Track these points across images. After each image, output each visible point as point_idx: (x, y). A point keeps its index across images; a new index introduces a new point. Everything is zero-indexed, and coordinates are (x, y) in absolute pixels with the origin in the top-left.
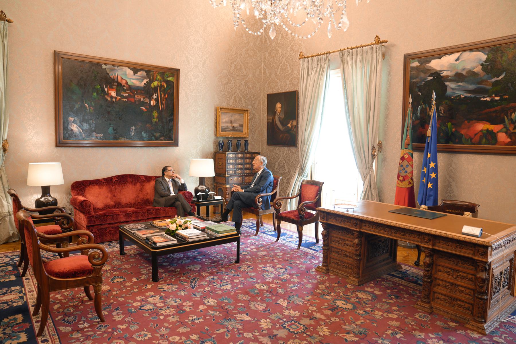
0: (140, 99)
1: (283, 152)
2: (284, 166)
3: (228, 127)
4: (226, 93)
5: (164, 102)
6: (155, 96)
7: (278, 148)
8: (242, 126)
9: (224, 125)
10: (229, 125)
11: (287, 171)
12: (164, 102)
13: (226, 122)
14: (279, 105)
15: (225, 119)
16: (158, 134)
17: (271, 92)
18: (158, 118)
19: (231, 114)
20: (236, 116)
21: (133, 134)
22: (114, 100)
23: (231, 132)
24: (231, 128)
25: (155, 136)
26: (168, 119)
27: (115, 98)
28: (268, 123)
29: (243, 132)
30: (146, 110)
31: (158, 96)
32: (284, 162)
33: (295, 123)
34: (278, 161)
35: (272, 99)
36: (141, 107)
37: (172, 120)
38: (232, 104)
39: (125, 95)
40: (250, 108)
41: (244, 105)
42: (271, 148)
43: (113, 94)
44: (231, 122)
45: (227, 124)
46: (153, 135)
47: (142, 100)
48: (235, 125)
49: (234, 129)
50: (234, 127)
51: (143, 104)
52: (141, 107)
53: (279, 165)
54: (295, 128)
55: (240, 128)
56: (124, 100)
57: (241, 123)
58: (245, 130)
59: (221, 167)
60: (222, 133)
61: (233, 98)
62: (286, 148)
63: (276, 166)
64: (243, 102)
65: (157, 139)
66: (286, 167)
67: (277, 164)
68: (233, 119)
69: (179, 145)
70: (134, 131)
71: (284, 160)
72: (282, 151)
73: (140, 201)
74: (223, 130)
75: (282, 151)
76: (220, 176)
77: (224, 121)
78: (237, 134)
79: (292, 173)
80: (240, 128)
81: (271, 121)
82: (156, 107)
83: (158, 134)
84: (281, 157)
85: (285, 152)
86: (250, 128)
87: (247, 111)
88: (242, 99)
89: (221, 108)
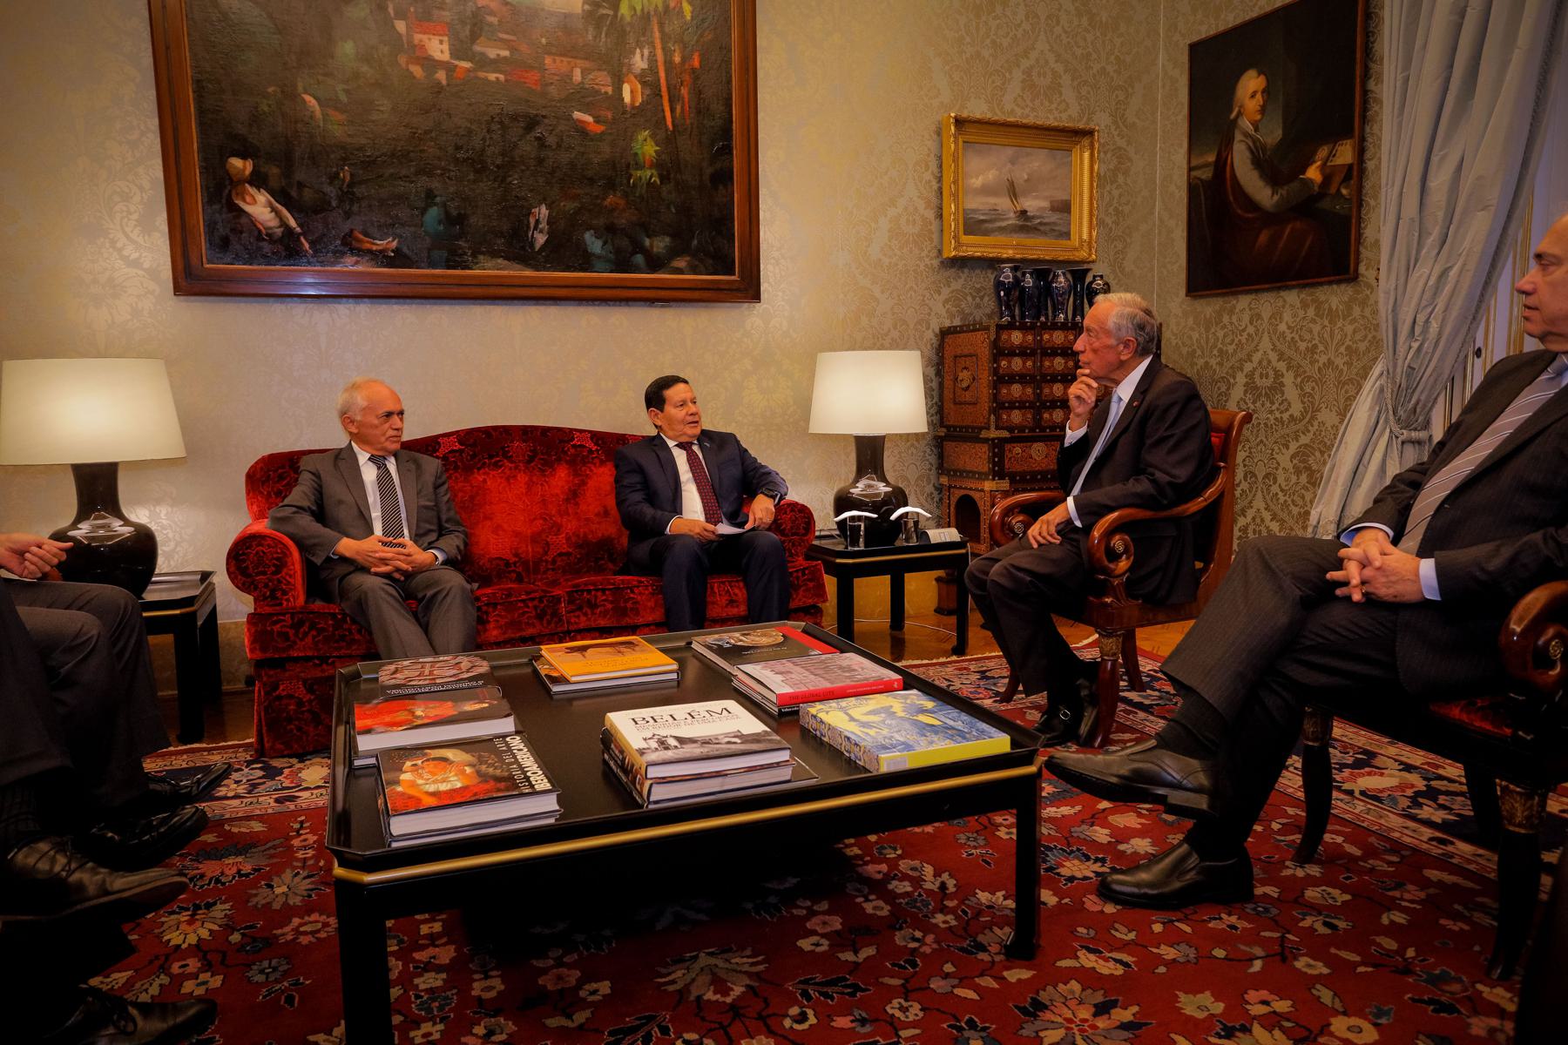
0: (570, 76)
1: (1277, 316)
2: (1278, 387)
3: (996, 215)
4: (986, 53)
5: (684, 91)
6: (639, 62)
7: (1243, 302)
8: (1064, 207)
9: (974, 203)
10: (1003, 203)
11: (1296, 408)
12: (684, 91)
13: (986, 190)
14: (1251, 85)
15: (984, 171)
16: (660, 245)
17: (1206, 30)
18: (658, 165)
19: (1010, 151)
20: (1037, 162)
21: (541, 239)
22: (441, 76)
23: (1015, 239)
24: (1012, 220)
25: (647, 254)
26: (709, 171)
27: (449, 68)
28: (1193, 189)
29: (1067, 235)
30: (600, 128)
31: (652, 60)
32: (1282, 366)
33: (1345, 154)
34: (1248, 367)
35: (1213, 65)
36: (577, 115)
37: (723, 177)
38: (1013, 108)
39: (492, 53)
40: (1101, 121)
41: (1074, 111)
42: (1209, 307)
43: (439, 48)
44: (1013, 192)
45: (992, 200)
46: (638, 248)
47: (577, 76)
48: (1032, 204)
49: (1026, 224)
50: (1024, 212)
51: (585, 98)
52: (577, 115)
53: (1250, 387)
54: (1347, 178)
55: (1053, 218)
56: (492, 77)
57: (1061, 196)
58: (1082, 227)
59: (968, 396)
60: (965, 239)
61: (1018, 75)
62: (1292, 297)
63: (1238, 392)
64: (1069, 94)
65: (655, 264)
66: (1291, 393)
67: (1241, 379)
68: (1020, 175)
69: (762, 297)
70: (544, 225)
71: (1281, 357)
72: (1266, 315)
73: (566, 549)
74: (973, 226)
75: (1266, 315)
76: (965, 439)
77: (977, 182)
78: (1039, 248)
79: (1327, 417)
80: (1053, 218)
81: (1206, 174)
82: (647, 114)
83: (660, 245)
84: (1265, 344)
85: (1287, 316)
86: (1101, 223)
87: (1090, 133)
88: (1066, 80)
89: (959, 122)
